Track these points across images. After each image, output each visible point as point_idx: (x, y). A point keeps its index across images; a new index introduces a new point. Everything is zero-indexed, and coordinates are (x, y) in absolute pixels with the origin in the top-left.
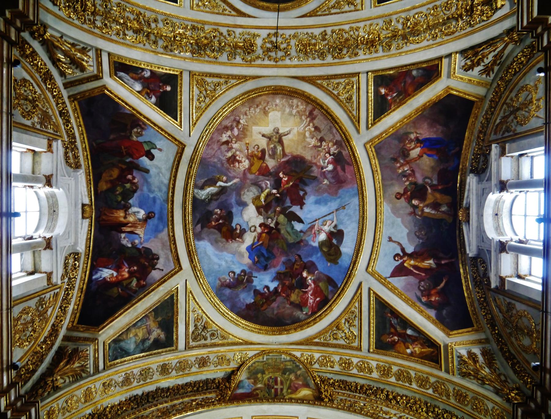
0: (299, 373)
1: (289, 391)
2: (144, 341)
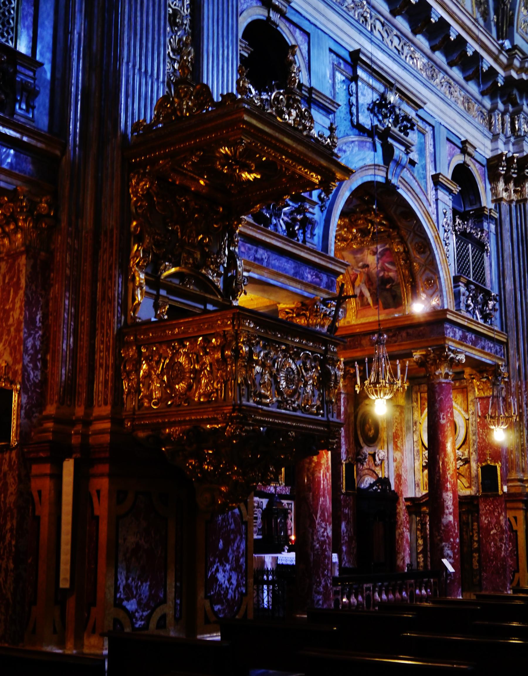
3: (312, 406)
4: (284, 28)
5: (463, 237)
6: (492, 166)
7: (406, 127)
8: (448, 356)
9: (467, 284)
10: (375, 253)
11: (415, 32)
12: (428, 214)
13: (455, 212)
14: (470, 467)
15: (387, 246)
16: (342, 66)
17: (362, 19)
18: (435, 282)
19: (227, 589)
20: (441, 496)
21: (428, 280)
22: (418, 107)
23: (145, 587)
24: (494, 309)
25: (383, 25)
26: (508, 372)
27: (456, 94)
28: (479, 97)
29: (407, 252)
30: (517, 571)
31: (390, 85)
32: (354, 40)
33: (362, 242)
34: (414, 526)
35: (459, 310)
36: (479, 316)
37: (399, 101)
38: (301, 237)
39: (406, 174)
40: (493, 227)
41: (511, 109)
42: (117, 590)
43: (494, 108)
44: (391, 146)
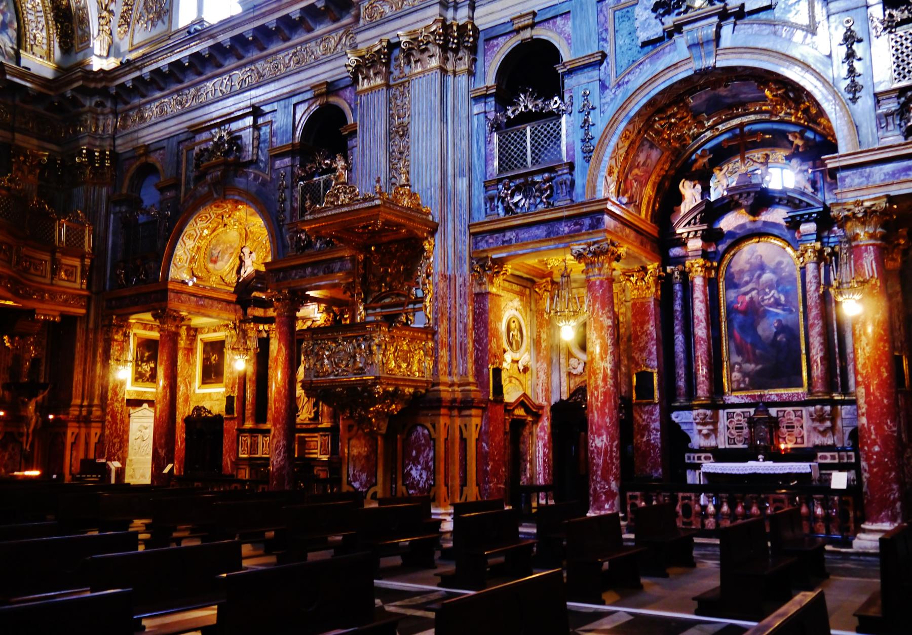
19: (419, 481)
23: (364, 476)
42: (348, 476)
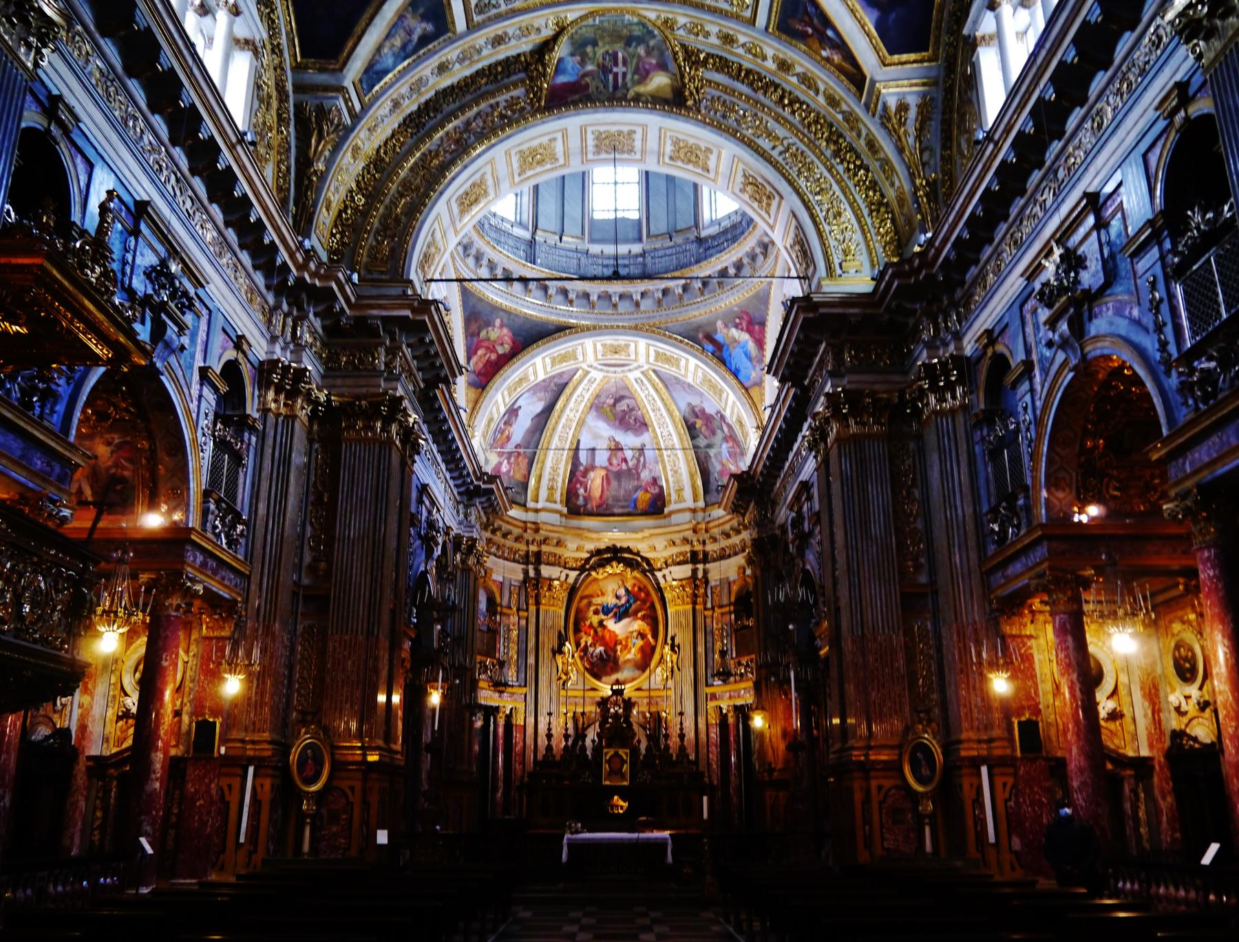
0: (652, 43)
1: (636, 77)
2: (404, 47)
3: (56, 639)
4: (63, 148)
5: (221, 445)
6: (265, 370)
7: (183, 304)
8: (184, 584)
9: (218, 502)
10: (109, 444)
11: (211, 200)
12: (188, 411)
13: (217, 416)
14: (180, 722)
15: (128, 439)
16: (123, 214)
17: (157, 166)
18: (182, 493)
20: (149, 755)
21: (173, 489)
22: (199, 284)
24: (242, 534)
25: (178, 180)
26: (246, 610)
27: (241, 281)
28: (264, 291)
29: (153, 451)
30: (223, 851)
31: (174, 251)
32: (144, 189)
33: (95, 427)
34: (93, 792)
35: (205, 531)
36: (224, 541)
37: (180, 273)
38: (37, 411)
39: (173, 360)
40: (254, 439)
41: (295, 313)
43: (277, 307)
44: (164, 325)
